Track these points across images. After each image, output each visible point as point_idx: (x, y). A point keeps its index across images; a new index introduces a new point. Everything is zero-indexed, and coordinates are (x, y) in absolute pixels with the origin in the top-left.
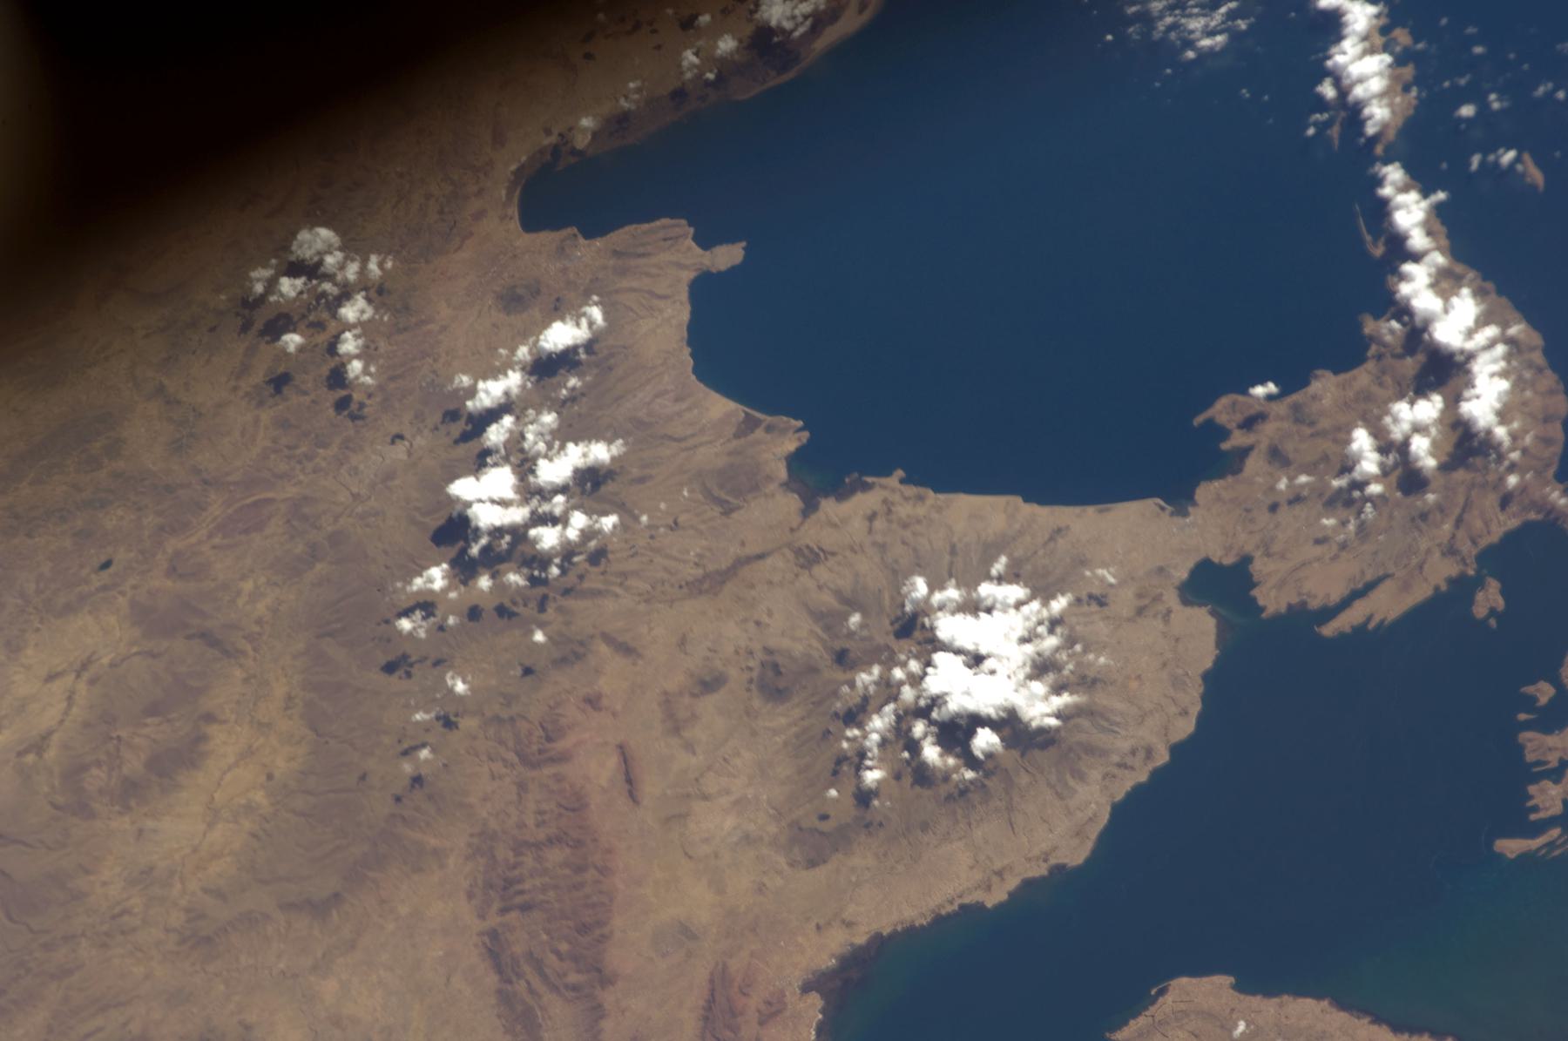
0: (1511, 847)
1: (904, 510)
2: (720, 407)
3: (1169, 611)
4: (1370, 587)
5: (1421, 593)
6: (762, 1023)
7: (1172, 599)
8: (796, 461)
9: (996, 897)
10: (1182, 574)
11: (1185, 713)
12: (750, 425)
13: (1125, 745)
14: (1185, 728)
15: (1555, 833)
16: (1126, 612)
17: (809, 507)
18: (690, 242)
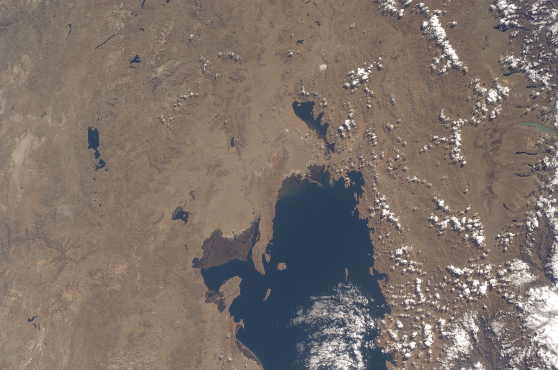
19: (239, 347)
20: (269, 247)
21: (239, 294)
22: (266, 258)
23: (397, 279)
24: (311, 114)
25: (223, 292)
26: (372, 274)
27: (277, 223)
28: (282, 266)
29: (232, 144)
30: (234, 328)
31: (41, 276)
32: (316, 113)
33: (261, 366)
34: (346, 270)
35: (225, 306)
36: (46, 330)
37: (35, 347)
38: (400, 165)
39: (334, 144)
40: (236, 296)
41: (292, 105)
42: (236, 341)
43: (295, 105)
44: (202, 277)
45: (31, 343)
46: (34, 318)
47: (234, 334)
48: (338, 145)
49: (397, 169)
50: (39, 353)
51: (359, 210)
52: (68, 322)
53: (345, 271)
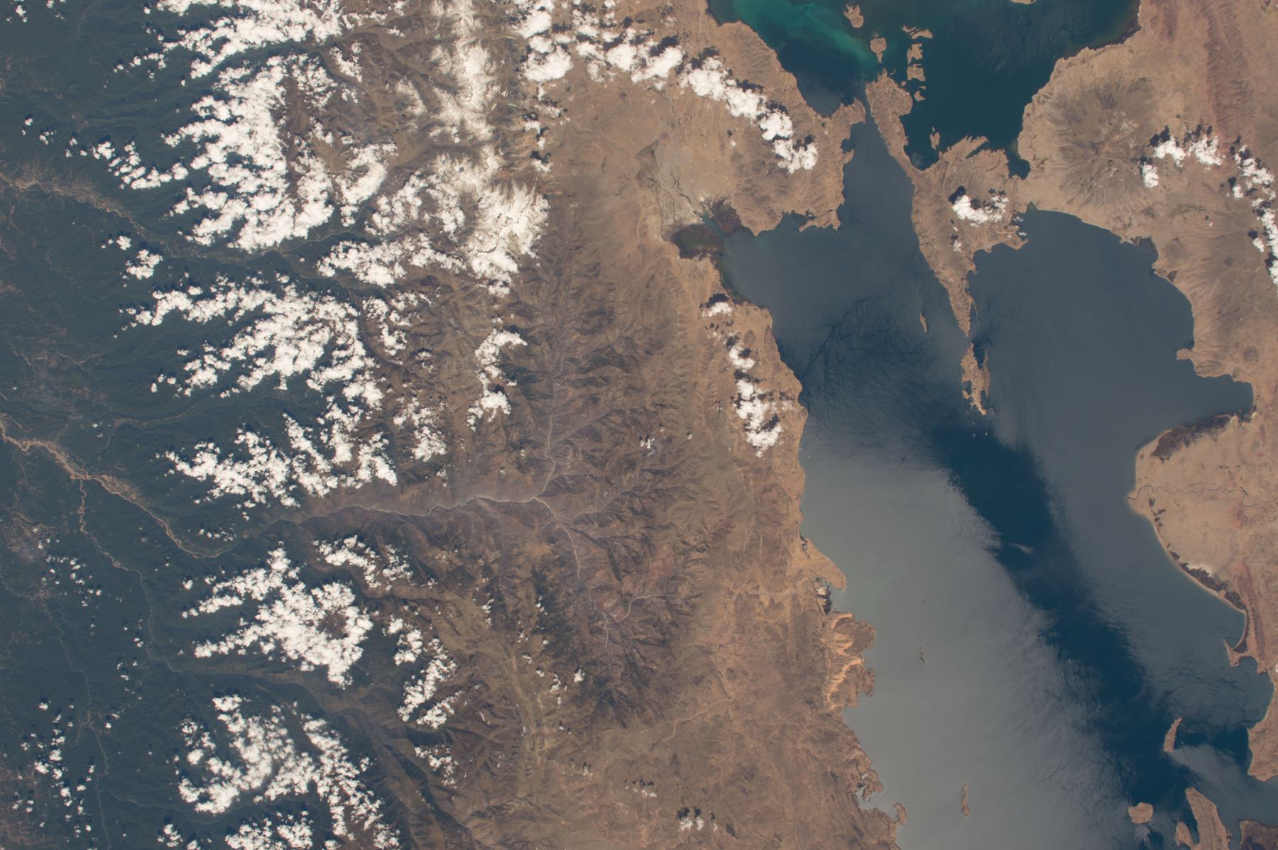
0: (927, 34)
1: (1119, 225)
2: (1181, 285)
3: (1034, 159)
4: (971, 155)
5: (957, 147)
6: (1157, 16)
7: (1033, 164)
8: (1154, 257)
9: (1086, 51)
10: (1030, 175)
11: (1028, 115)
12: (1171, 276)
13: (1046, 106)
14: (1028, 108)
15: (915, 37)
16: (1047, 162)
18: (1196, 364)
22: (1187, 833)
23: (833, 797)
30: (1252, 642)
33: (1166, 550)
40: (1258, 727)
42: (1244, 607)
47: (1252, 627)
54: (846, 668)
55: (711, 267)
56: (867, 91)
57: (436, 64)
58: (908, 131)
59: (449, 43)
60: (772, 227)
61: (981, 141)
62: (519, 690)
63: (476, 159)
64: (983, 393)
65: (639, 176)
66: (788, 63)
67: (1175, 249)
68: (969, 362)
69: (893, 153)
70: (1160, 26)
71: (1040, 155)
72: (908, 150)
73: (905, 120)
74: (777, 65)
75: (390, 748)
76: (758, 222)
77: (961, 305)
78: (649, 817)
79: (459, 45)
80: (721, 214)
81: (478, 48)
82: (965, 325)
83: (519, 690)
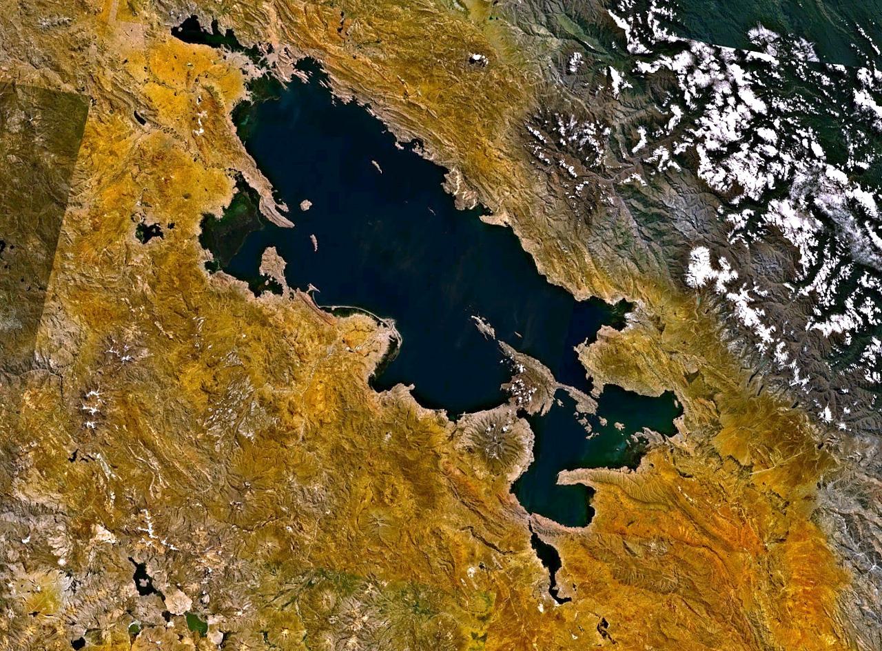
0: (589, 437)
2: (430, 412)
5: (550, 405)
7: (517, 418)
8: (447, 415)
9: (527, 470)
14: (534, 436)
17: (456, 422)
19: (329, 311)
20: (276, 197)
21: (284, 263)
24: (202, 30)
25: (266, 274)
26: (402, 148)
27: (264, 168)
28: (306, 205)
29: (143, 122)
31: (40, 409)
32: (206, 25)
34: (374, 162)
35: (280, 285)
36: (102, 455)
37: (105, 479)
38: (342, 23)
39: (255, 47)
41: (172, 34)
43: (175, 32)
44: (230, 276)
45: (97, 478)
46: (75, 454)
48: (260, 45)
49: (342, 29)
50: (115, 480)
51: (339, 96)
52: (120, 427)
53: (374, 165)
54: (458, 188)
55: (611, 303)
56: (596, 404)
57: (760, 310)
58: (572, 399)
59: (761, 318)
60: (600, 332)
61: (542, 415)
62: (579, 100)
63: (725, 284)
64: (478, 323)
65: (659, 319)
66: (632, 394)
67: (441, 422)
68: (492, 332)
69: (573, 388)
70: (505, 498)
71: (517, 423)
72: (568, 393)
73: (577, 403)
74: (635, 390)
75: (605, 54)
76: (605, 331)
77: (510, 351)
78: (497, 83)
79: (758, 321)
80: (620, 324)
81: (750, 325)
82: (502, 343)
83: (579, 100)
